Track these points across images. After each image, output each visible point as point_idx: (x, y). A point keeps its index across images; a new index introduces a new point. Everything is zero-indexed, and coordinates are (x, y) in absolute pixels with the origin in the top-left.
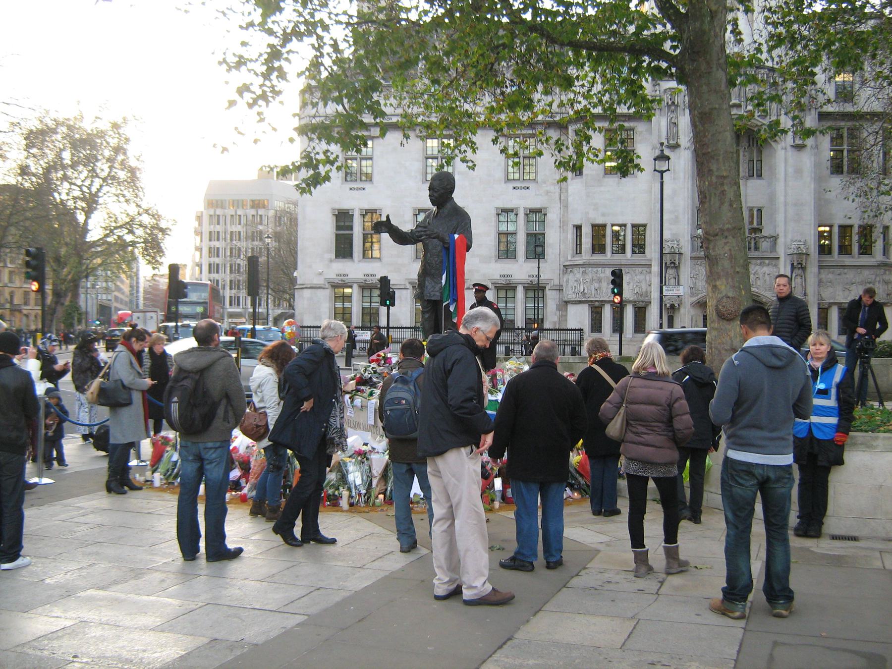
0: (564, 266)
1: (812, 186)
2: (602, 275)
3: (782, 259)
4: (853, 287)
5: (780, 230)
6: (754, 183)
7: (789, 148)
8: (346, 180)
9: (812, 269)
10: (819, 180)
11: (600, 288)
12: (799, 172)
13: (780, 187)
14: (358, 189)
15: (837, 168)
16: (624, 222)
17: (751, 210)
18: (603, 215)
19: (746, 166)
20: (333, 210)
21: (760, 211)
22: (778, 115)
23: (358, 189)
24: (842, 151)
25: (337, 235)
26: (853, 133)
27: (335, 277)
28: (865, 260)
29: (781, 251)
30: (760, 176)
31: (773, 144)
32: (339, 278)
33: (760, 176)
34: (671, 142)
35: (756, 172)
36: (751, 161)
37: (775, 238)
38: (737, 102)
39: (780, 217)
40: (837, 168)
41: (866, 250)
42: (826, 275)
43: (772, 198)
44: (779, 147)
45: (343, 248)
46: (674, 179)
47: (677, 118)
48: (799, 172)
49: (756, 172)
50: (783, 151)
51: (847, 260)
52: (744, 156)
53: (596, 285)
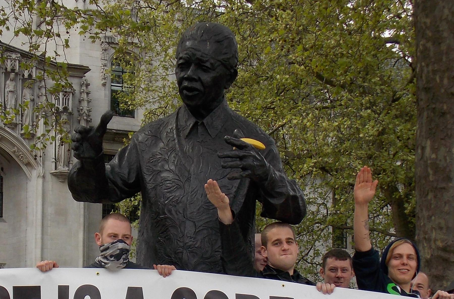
7: (49, 177)
44: (35, 173)
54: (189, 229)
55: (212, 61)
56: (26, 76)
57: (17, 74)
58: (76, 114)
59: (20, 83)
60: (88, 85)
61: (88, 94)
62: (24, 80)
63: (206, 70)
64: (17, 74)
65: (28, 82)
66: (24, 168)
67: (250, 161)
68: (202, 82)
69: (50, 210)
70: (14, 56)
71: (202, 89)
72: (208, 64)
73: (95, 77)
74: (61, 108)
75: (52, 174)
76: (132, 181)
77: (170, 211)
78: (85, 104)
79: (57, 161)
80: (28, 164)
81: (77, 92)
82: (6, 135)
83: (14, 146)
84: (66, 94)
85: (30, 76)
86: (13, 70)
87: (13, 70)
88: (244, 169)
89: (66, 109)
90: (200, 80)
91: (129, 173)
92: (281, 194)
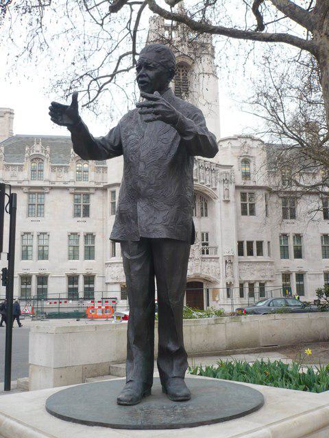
0: (106, 264)
3: (221, 258)
4: (255, 272)
5: (219, 244)
6: (204, 219)
9: (236, 264)
10: (237, 218)
12: (227, 214)
13: (218, 223)
15: (244, 213)
17: (203, 234)
21: (207, 234)
24: (246, 204)
26: (252, 194)
28: (260, 258)
29: (219, 255)
33: (206, 215)
35: (204, 213)
36: (202, 208)
37: (216, 248)
39: (219, 237)
40: (244, 213)
41: (260, 253)
42: (244, 267)
43: (213, 227)
48: (227, 214)
49: (204, 213)
51: (251, 258)
54: (142, 166)
55: (154, 63)
63: (150, 69)
67: (160, 108)
68: (149, 77)
69: (223, 213)
71: (150, 81)
72: (151, 65)
73: (236, 168)
76: (116, 145)
77: (132, 158)
80: (215, 198)
88: (156, 113)
90: (147, 75)
91: (115, 141)
92: (190, 133)
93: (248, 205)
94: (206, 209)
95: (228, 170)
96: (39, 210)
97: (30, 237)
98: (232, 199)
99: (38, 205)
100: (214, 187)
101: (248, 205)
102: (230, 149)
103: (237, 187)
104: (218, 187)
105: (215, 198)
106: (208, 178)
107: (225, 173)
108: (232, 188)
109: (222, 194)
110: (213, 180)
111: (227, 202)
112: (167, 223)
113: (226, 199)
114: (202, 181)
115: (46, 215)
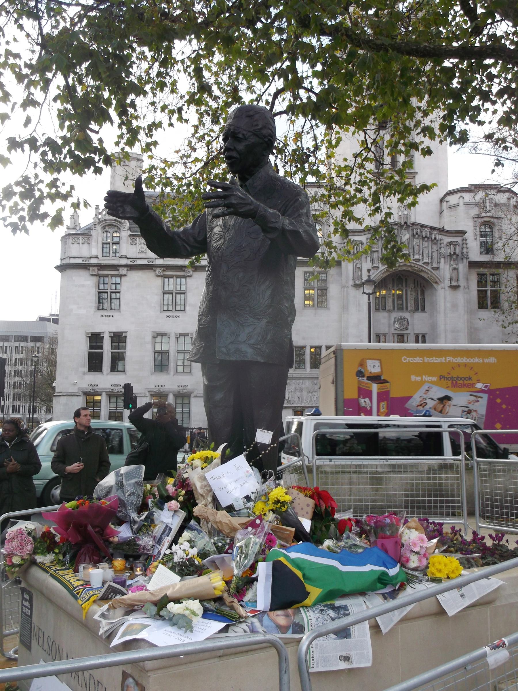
1: (466, 317)
2: (303, 386)
6: (419, 316)
7: (447, 288)
8: (98, 309)
10: (471, 313)
11: (301, 396)
14: (108, 316)
15: (482, 305)
16: (320, 345)
18: (304, 338)
19: (413, 302)
20: (87, 332)
22: (438, 263)
23: (108, 316)
24: (486, 291)
25: (90, 354)
27: (87, 387)
30: (423, 310)
31: (435, 285)
32: (91, 387)
33: (423, 310)
34: (357, 282)
36: (416, 299)
38: (407, 252)
40: (482, 305)
44: (440, 287)
45: (95, 364)
46: (359, 311)
47: (361, 264)
48: (455, 306)
49: (420, 306)
50: (443, 290)
52: (411, 294)
53: (298, 394)
56: (433, 238)
57: (428, 238)
58: (460, 255)
59: (430, 242)
60: (466, 240)
61: (467, 244)
62: (432, 240)
64: (428, 238)
65: (435, 241)
66: (435, 285)
69: (448, 305)
70: (426, 229)
73: (469, 235)
74: (452, 253)
75: (450, 287)
78: (465, 250)
79: (451, 279)
80: (436, 283)
81: (461, 244)
82: (424, 269)
83: (428, 274)
84: (455, 245)
85: (435, 238)
86: (426, 236)
87: (426, 236)
89: (455, 253)
93: (489, 293)
94: (423, 299)
95: (458, 239)
96: (178, 301)
97: (165, 339)
98: (462, 282)
99: (176, 293)
100: (435, 265)
101: (489, 293)
102: (462, 208)
103: (473, 265)
104: (442, 265)
105: (436, 283)
106: (426, 252)
107: (450, 243)
108: (463, 267)
109: (448, 276)
110: (435, 255)
111: (455, 288)
112: (252, 341)
113: (454, 283)
114: (417, 257)
115: (188, 308)
